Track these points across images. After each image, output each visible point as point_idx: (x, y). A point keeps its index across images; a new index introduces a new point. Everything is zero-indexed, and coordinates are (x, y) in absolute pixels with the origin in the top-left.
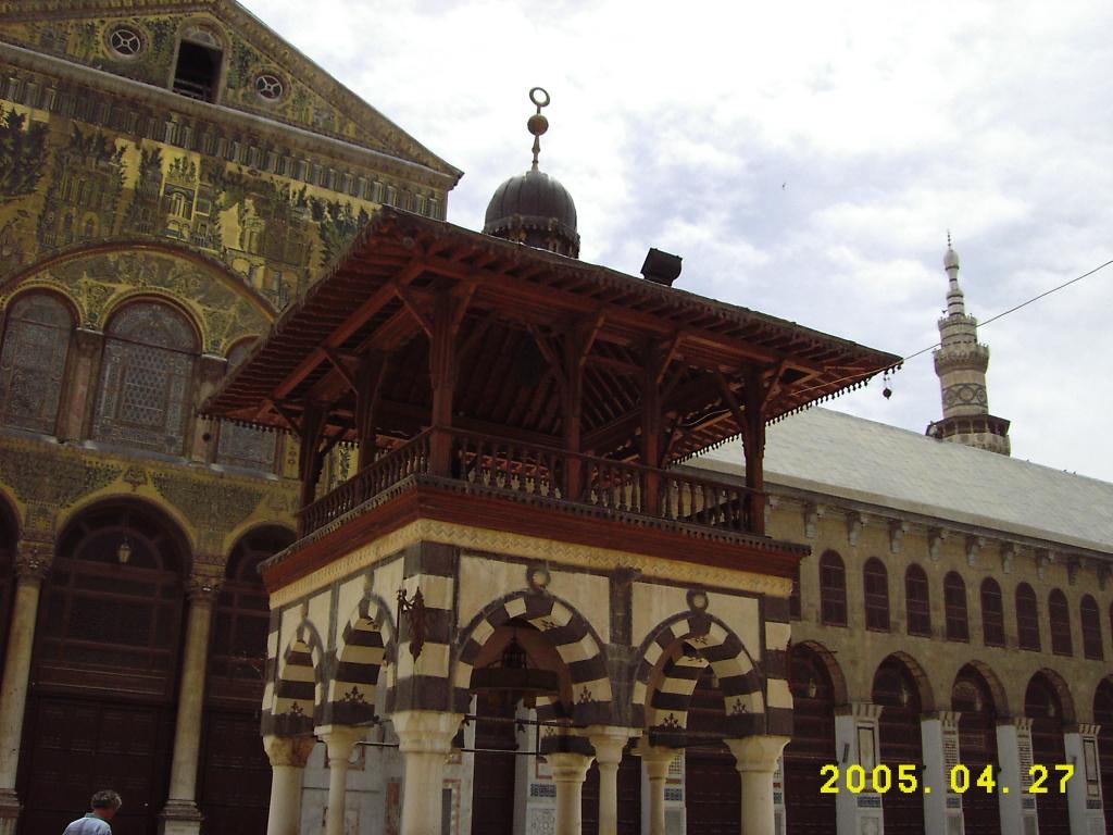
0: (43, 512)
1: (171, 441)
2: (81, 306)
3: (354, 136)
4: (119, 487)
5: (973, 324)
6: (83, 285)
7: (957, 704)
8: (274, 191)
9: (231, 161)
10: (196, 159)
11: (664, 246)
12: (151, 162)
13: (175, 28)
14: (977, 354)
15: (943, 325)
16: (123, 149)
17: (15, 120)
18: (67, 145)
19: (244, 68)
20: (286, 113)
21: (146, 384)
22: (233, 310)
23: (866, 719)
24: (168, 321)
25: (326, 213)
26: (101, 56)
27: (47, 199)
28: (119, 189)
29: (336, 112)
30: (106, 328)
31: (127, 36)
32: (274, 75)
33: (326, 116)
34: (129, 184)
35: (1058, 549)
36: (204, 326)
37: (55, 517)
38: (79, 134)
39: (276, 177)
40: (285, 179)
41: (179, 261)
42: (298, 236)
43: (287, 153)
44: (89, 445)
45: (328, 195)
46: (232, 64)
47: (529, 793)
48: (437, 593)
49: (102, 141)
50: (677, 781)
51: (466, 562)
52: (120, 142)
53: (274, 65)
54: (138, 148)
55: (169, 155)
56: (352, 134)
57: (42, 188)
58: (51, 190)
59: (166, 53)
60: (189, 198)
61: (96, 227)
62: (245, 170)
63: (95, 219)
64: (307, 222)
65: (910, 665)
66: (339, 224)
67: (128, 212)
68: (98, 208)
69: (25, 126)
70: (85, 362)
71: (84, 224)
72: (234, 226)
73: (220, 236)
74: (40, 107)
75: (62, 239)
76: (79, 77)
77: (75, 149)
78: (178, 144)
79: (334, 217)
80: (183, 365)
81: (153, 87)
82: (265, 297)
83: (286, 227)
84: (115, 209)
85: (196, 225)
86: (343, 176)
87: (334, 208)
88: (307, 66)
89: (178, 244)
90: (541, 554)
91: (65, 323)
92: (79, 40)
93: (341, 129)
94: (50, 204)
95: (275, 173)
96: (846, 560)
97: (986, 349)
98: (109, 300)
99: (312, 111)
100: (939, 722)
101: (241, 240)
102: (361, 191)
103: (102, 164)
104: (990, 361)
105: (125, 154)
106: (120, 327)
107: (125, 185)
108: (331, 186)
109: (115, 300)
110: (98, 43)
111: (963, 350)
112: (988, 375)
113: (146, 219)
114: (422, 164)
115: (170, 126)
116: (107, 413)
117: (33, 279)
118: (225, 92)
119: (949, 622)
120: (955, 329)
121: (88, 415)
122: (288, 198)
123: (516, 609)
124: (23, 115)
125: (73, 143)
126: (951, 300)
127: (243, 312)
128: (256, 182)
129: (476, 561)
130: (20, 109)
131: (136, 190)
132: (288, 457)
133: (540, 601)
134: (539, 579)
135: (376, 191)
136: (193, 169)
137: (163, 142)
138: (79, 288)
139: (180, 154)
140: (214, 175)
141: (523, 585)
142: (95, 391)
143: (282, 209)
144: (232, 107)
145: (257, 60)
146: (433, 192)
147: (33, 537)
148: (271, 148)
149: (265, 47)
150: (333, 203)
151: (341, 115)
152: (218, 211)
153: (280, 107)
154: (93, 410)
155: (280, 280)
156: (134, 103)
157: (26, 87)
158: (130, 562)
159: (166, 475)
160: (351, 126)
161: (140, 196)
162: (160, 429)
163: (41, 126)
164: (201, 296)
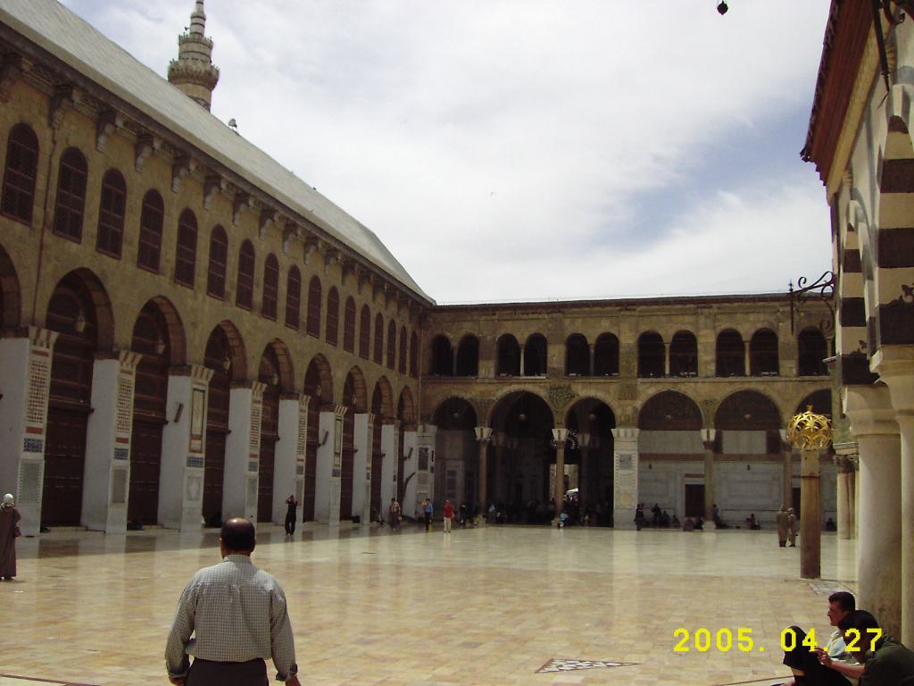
5: (210, 46)
7: (263, 378)
14: (210, 74)
15: (183, 41)
23: (200, 381)
35: (346, 252)
47: (22, 447)
50: (38, 431)
65: (229, 335)
96: (199, 222)
97: (218, 72)
100: (250, 391)
104: (218, 83)
111: (199, 67)
112: (215, 93)
119: (265, 299)
120: (195, 47)
126: (195, 20)
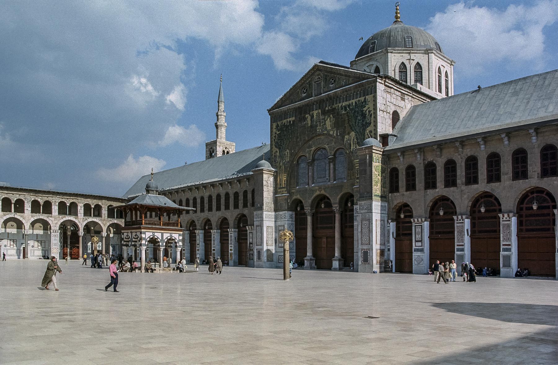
1: (327, 179)
4: (318, 193)
10: (320, 111)
12: (312, 117)
24: (324, 151)
36: (328, 150)
41: (322, 137)
43: (337, 97)
45: (347, 103)
52: (307, 116)
55: (315, 113)
66: (351, 110)
72: (328, 123)
87: (349, 106)
127: (335, 143)
139: (317, 112)
140: (324, 113)
143: (338, 113)
154: (313, 178)
158: (325, 207)
161: (311, 126)
162: (325, 177)
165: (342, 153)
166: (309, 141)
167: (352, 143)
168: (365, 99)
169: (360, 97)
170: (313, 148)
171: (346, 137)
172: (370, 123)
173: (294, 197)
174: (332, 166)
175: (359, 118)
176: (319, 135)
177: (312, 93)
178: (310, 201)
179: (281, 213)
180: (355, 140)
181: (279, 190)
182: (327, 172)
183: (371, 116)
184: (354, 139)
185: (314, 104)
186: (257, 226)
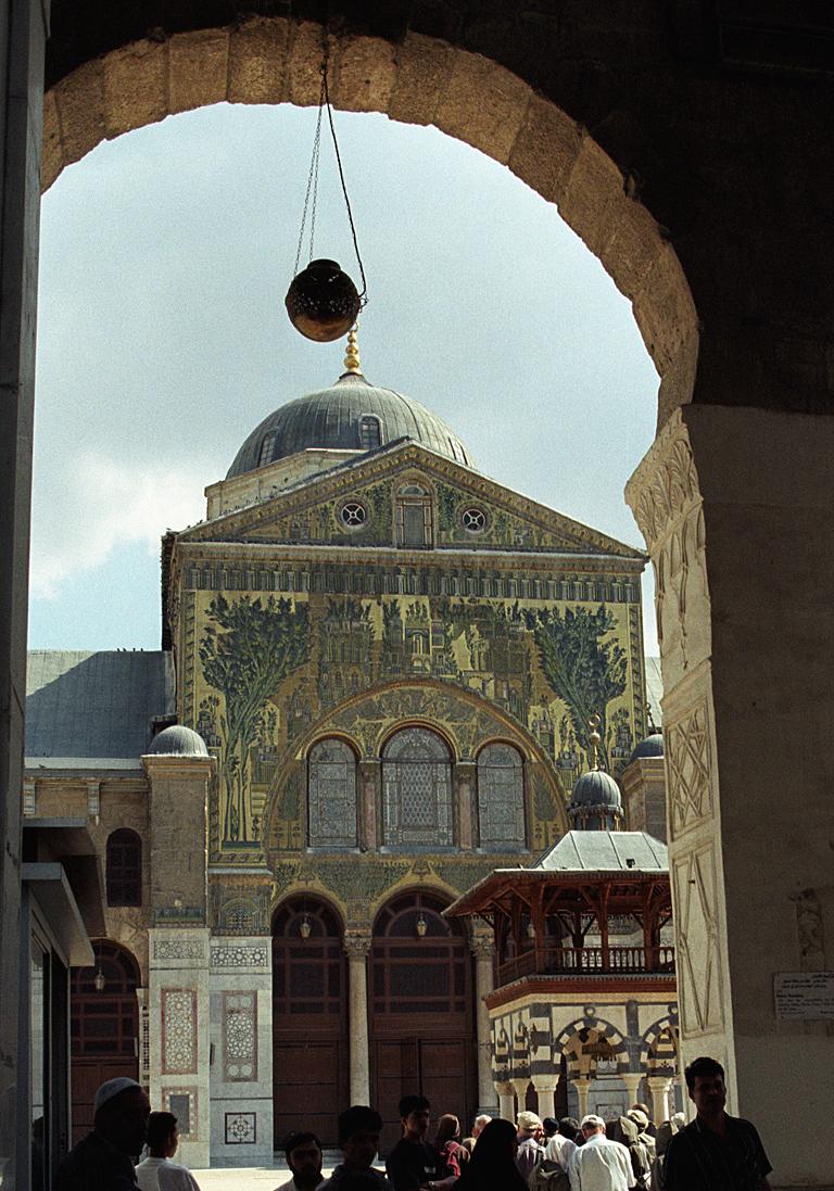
0: (359, 906)
1: (443, 836)
2: (358, 741)
3: (552, 544)
4: (410, 880)
6: (358, 727)
8: (492, 612)
9: (453, 595)
10: (425, 601)
11: (630, 858)
12: (391, 613)
13: (389, 491)
16: (368, 608)
17: (285, 605)
18: (326, 615)
19: (451, 509)
20: (491, 540)
21: (418, 794)
22: (475, 719)
24: (426, 739)
25: (537, 621)
26: (337, 533)
27: (320, 665)
28: (371, 643)
29: (533, 526)
30: (381, 755)
31: (353, 508)
32: (475, 508)
33: (525, 532)
34: (378, 637)
36: (454, 739)
37: (368, 909)
38: (333, 604)
39: (491, 600)
40: (498, 600)
41: (427, 690)
42: (516, 646)
43: (498, 576)
44: (383, 850)
45: (537, 604)
46: (440, 508)
48: (542, 1024)
49: (351, 605)
51: (554, 1009)
52: (365, 603)
53: (475, 499)
54: (379, 604)
55: (404, 603)
56: (550, 544)
57: (313, 656)
58: (321, 656)
59: (386, 514)
60: (427, 637)
61: (359, 678)
62: (466, 599)
63: (358, 671)
64: (523, 633)
67: (381, 660)
68: (358, 663)
69: (293, 609)
70: (370, 785)
71: (350, 678)
73: (454, 662)
74: (300, 590)
75: (336, 693)
76: (323, 558)
77: (333, 618)
78: (409, 593)
79: (545, 623)
80: (443, 772)
81: (380, 549)
82: (499, 706)
83: (506, 641)
84: (371, 660)
85: (434, 656)
86: (547, 583)
87: (544, 614)
88: (502, 491)
89: (424, 677)
90: (589, 1001)
91: (350, 756)
92: (318, 524)
93: (540, 541)
94: (322, 669)
95: (491, 596)
98: (380, 732)
99: (513, 532)
101: (472, 662)
102: (564, 593)
103: (355, 624)
105: (371, 611)
106: (394, 749)
107: (375, 639)
108: (539, 596)
109: (384, 732)
110: (332, 522)
113: (395, 662)
114: (613, 554)
115: (400, 578)
116: (393, 822)
117: (321, 729)
118: (439, 535)
121: (379, 826)
122: (504, 615)
123: (580, 1026)
124: (289, 600)
125: (331, 612)
127: (483, 721)
128: (476, 608)
129: (559, 1008)
130: (286, 596)
131: (384, 639)
132: (535, 833)
133: (590, 1021)
134: (590, 1012)
135: (577, 589)
136: (425, 611)
137: (397, 593)
138: (356, 729)
139: (412, 600)
140: (442, 610)
141: (582, 1015)
142: (381, 806)
143: (500, 626)
144: (447, 548)
145: (460, 498)
146: (627, 578)
147: (355, 926)
148: (483, 575)
149: (464, 485)
150: (542, 610)
151: (538, 528)
152: (450, 642)
153: (485, 536)
155: (508, 688)
156: (370, 567)
157: (287, 576)
158: (426, 935)
159: (443, 863)
160: (548, 536)
161: (387, 644)
162: (435, 827)
163: (304, 606)
164: (449, 715)
165: (504, 758)
166: (373, 690)
167: (557, 736)
168: (602, 609)
169: (585, 599)
170: (386, 722)
171: (535, 711)
172: (623, 688)
173: (296, 886)
174: (465, 792)
175: (582, 661)
176: (421, 680)
177: (389, 532)
178: (374, 907)
179: (236, 942)
180: (569, 726)
181: (226, 852)
182: (444, 813)
183: (624, 665)
184: (563, 724)
185: (399, 572)
186: (164, 991)
